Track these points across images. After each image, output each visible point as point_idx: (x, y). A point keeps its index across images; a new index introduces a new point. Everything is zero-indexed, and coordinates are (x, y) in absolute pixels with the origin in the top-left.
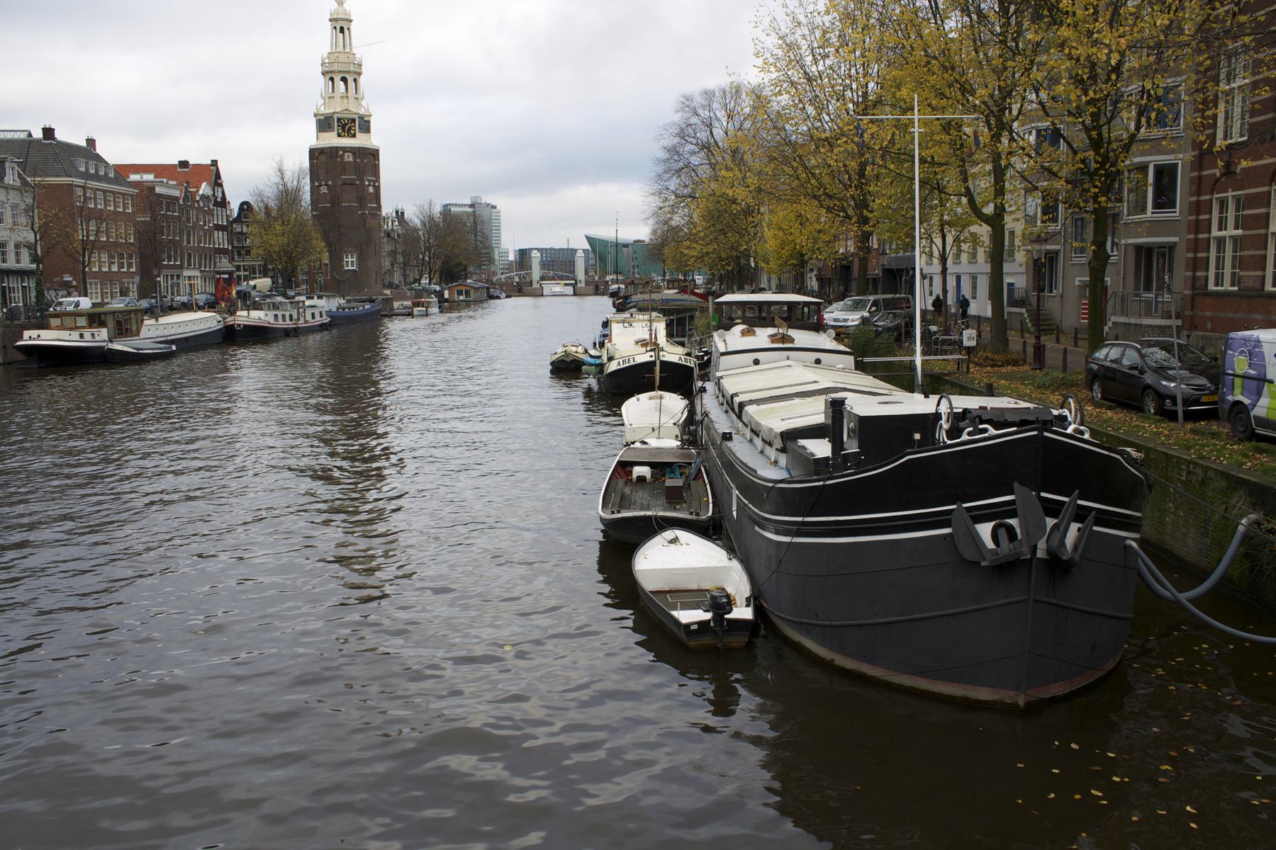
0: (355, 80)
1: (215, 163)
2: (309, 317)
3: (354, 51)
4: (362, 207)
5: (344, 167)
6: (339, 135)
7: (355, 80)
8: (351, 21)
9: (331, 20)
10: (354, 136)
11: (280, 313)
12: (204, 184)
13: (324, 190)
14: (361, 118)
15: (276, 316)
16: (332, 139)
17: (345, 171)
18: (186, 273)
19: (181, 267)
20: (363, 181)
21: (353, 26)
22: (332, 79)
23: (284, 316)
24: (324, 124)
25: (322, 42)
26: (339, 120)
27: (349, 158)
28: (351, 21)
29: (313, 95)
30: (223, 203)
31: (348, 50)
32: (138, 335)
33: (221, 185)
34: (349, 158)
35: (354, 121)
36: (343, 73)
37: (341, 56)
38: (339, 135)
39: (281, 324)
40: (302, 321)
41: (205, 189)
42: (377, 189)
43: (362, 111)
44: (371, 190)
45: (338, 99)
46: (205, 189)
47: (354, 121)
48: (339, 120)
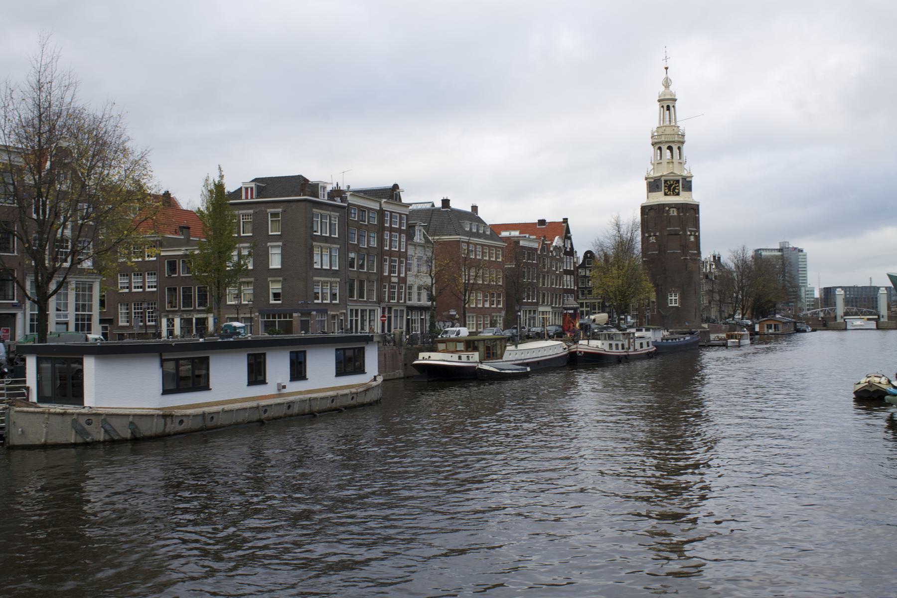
0: (679, 148)
1: (565, 220)
2: (638, 346)
3: (678, 124)
4: (684, 253)
5: (670, 220)
6: (666, 194)
7: (679, 148)
8: (675, 100)
9: (659, 101)
10: (678, 194)
11: (614, 343)
12: (557, 238)
13: (653, 240)
14: (684, 179)
15: (611, 345)
16: (660, 198)
17: (670, 223)
18: (541, 309)
19: (537, 304)
20: (685, 232)
21: (677, 104)
22: (660, 148)
23: (617, 345)
24: (654, 185)
25: (650, 118)
26: (666, 181)
27: (674, 212)
28: (675, 100)
29: (645, 162)
30: (571, 253)
31: (673, 124)
33: (570, 238)
34: (674, 212)
35: (678, 181)
36: (669, 143)
37: (667, 129)
39: (614, 352)
40: (632, 349)
41: (557, 241)
42: (697, 238)
43: (685, 174)
44: (692, 239)
45: (665, 164)
46: (557, 241)
47: (678, 181)
48: (666, 181)
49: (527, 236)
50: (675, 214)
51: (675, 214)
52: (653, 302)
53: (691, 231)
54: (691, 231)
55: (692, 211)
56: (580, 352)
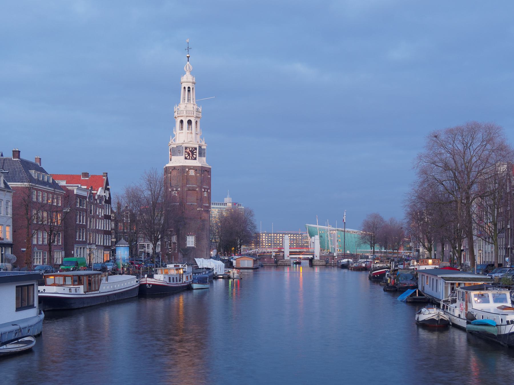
6: (186, 158)
10: (195, 159)
27: (192, 173)
32: (98, 290)
38: (186, 158)
41: (100, 192)
42: (209, 194)
44: (206, 194)
46: (100, 192)
47: (196, 149)
48: (186, 148)
49: (79, 185)
50: (193, 174)
51: (193, 174)
52: (174, 243)
53: (205, 189)
54: (205, 189)
55: (206, 172)
56: (149, 284)
